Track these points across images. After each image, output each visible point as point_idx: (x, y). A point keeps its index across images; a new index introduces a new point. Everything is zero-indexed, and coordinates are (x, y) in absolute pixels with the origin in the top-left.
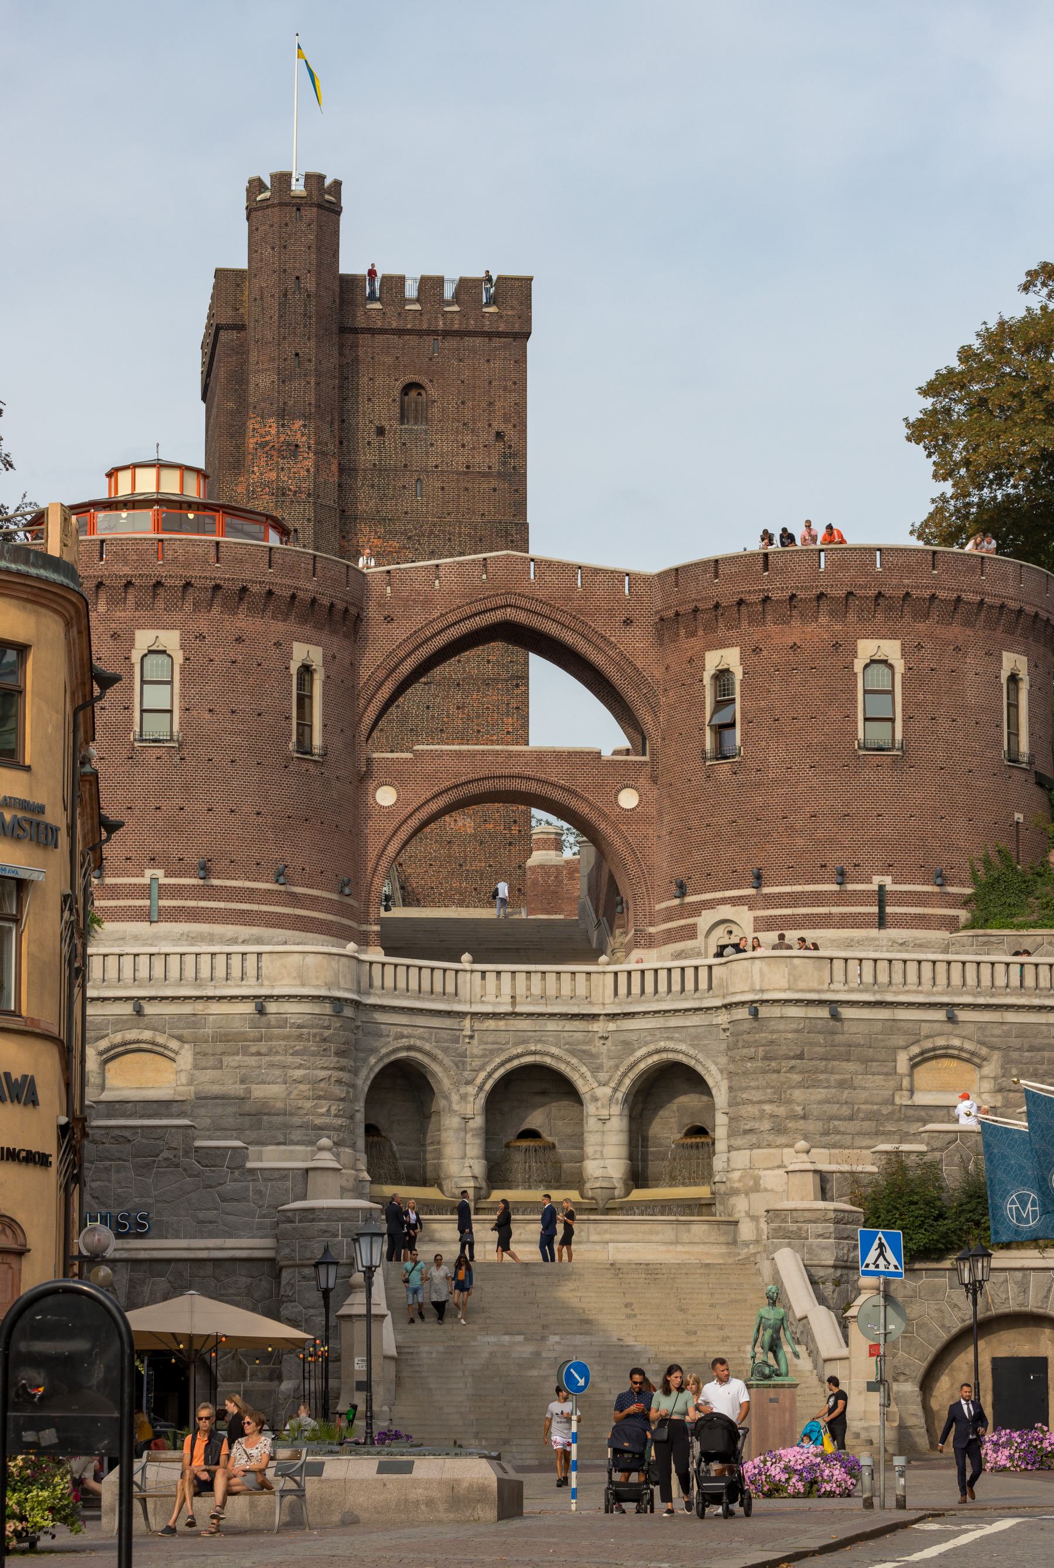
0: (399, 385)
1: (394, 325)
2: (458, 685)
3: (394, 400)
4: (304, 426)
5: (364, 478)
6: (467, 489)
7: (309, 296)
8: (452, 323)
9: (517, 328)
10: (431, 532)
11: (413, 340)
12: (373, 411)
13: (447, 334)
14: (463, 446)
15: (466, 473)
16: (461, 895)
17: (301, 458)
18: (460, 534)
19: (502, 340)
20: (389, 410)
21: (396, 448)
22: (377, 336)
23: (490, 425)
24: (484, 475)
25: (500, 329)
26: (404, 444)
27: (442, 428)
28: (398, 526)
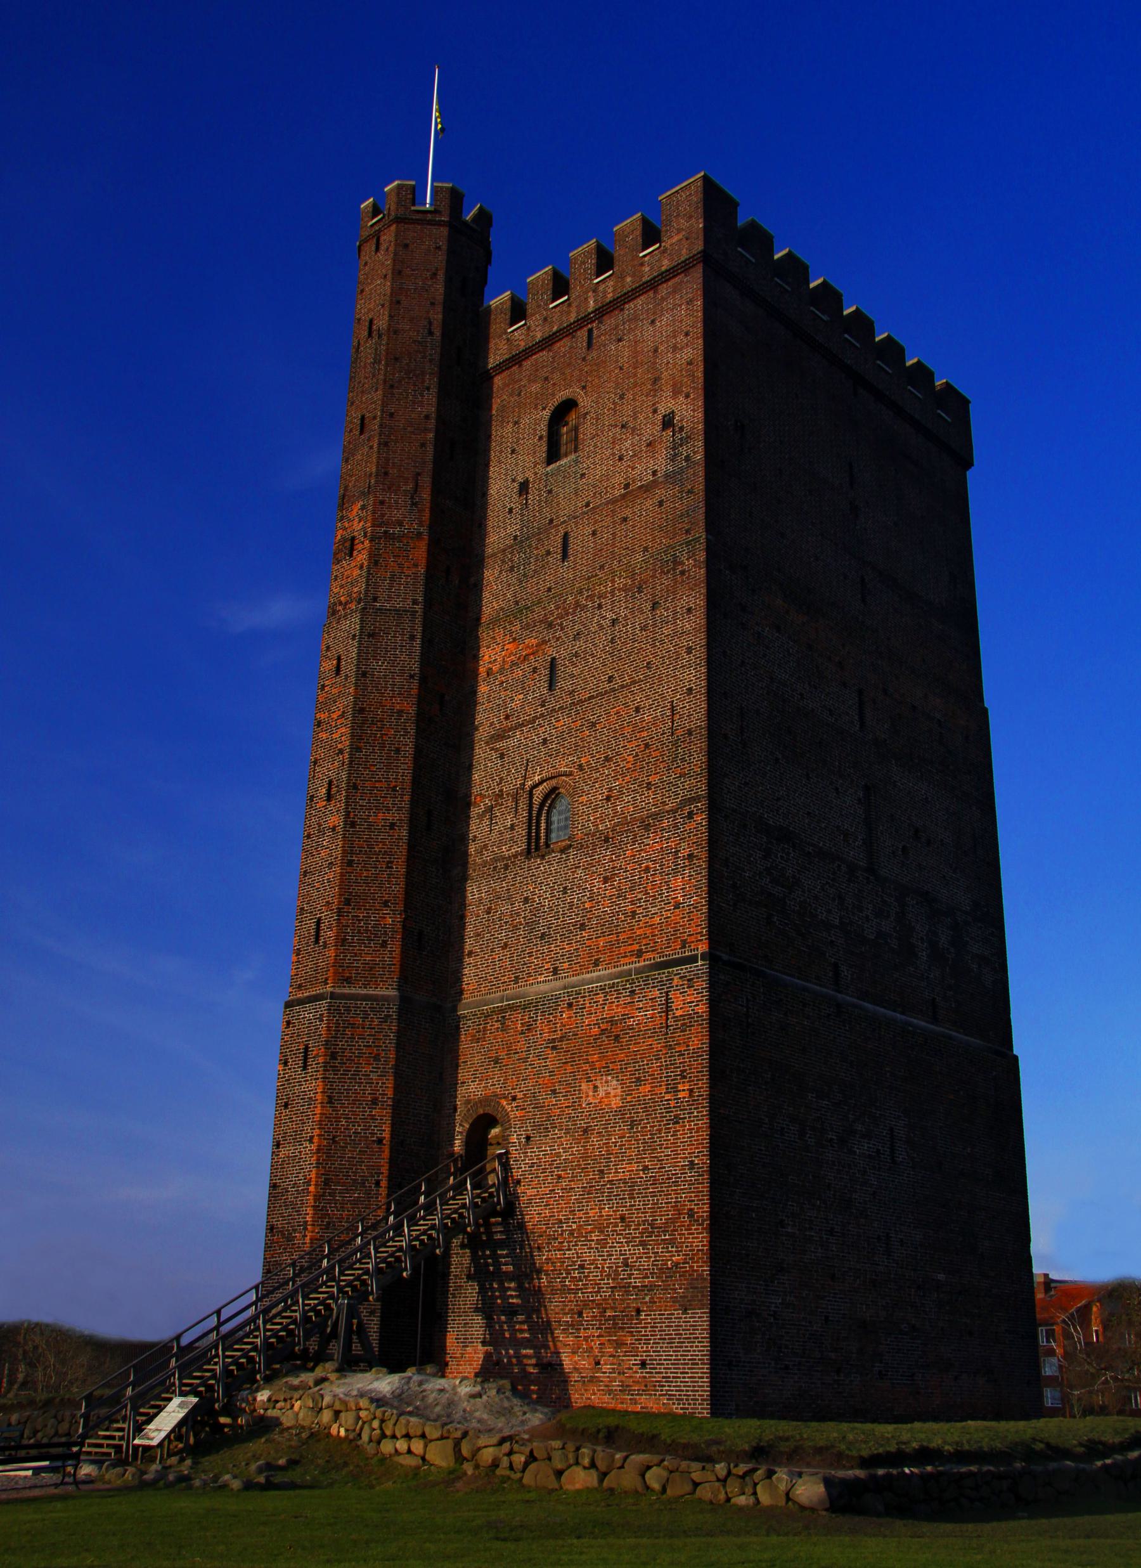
0: (547, 414)
1: (539, 336)
2: (606, 840)
3: (541, 438)
4: (363, 508)
5: (503, 561)
6: (625, 520)
7: (380, 336)
8: (605, 292)
9: (684, 254)
10: (577, 604)
11: (563, 346)
12: (517, 465)
13: (602, 312)
14: (621, 459)
15: (623, 496)
16: (602, 1232)
17: (355, 553)
18: (612, 592)
19: (670, 283)
20: (535, 453)
21: (540, 501)
22: (525, 363)
23: (655, 411)
24: (647, 488)
25: (663, 269)
26: (550, 492)
27: (596, 446)
28: (538, 613)
